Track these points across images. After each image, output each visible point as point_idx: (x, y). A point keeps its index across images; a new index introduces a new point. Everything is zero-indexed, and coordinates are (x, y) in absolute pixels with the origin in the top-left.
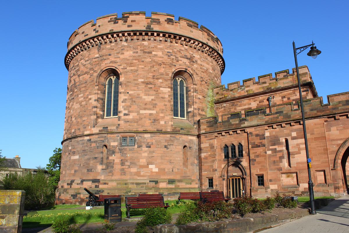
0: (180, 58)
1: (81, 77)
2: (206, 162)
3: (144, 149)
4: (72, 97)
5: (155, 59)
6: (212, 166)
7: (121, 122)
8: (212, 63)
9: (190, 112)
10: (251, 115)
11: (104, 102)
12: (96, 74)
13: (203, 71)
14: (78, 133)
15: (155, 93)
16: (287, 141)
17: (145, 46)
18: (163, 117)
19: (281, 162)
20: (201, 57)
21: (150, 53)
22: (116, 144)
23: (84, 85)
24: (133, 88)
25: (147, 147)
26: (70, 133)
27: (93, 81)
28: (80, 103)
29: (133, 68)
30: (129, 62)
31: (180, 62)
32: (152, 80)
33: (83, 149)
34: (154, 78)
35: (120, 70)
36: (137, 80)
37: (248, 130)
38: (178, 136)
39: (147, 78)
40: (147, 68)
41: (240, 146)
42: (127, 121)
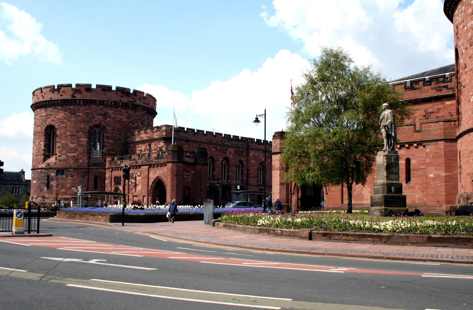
0: (95, 116)
3: (70, 178)
8: (127, 113)
13: (116, 122)
17: (72, 109)
18: (82, 158)
20: (114, 112)
21: (75, 114)
24: (63, 139)
29: (64, 125)
30: (62, 121)
31: (96, 119)
32: (75, 133)
39: (73, 132)
42: (60, 161)
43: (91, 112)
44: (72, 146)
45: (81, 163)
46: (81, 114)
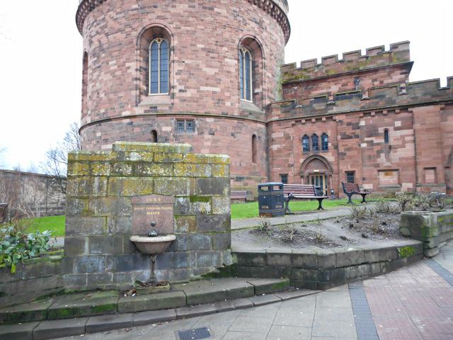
0: (248, 21)
1: (109, 37)
2: (280, 156)
3: (207, 136)
4: (98, 65)
5: (219, 19)
6: (288, 161)
7: (176, 101)
9: (257, 93)
10: (343, 99)
11: (148, 73)
12: (135, 34)
14: (110, 115)
15: (219, 64)
16: (386, 131)
18: (229, 97)
19: (379, 156)
21: (212, 9)
22: (168, 129)
23: (118, 48)
25: (210, 134)
26: (98, 115)
27: (131, 42)
28: (113, 73)
29: (189, 28)
30: (184, 19)
32: (215, 47)
33: (121, 135)
34: (217, 45)
35: (171, 28)
36: (195, 45)
37: (337, 118)
38: (246, 123)
39: (209, 44)
40: (208, 31)
41: (324, 135)
42: (184, 100)
43: (240, 11)
44: (211, 72)
45: (228, 108)
46: (224, 12)
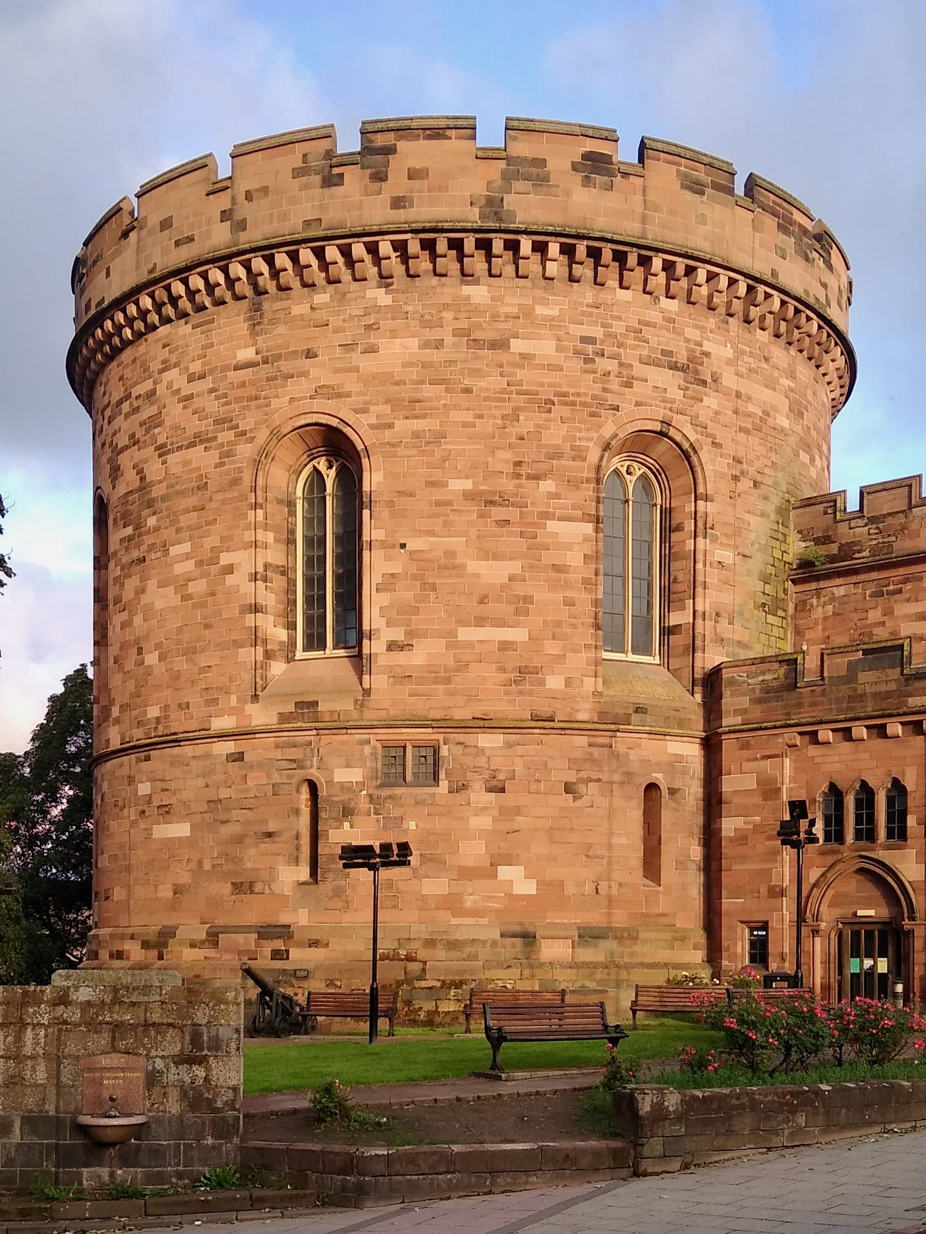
3: (479, 796)
17: (477, 310)
21: (500, 345)
29: (418, 425)
30: (405, 392)
32: (508, 485)
